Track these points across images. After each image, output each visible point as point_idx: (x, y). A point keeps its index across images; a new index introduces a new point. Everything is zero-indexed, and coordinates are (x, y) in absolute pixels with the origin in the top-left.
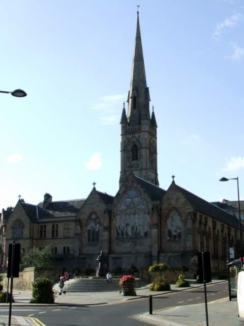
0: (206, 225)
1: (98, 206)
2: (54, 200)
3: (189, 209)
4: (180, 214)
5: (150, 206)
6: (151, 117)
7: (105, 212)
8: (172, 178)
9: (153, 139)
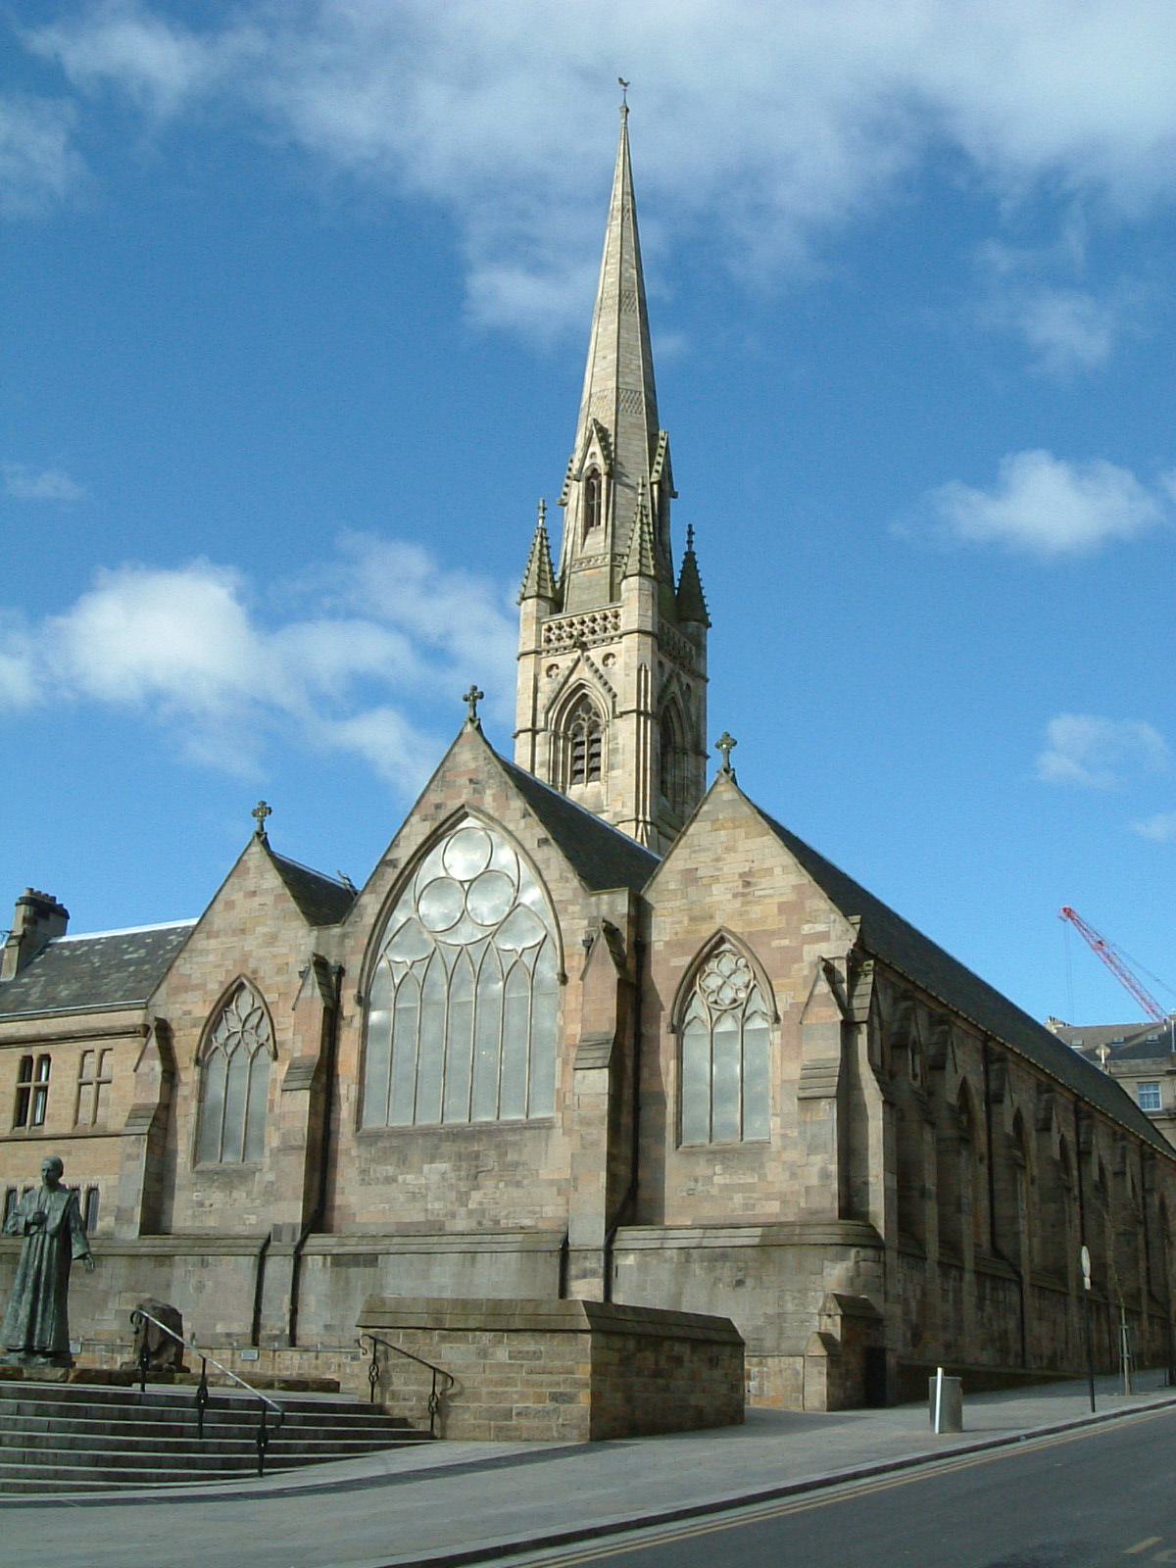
0: (937, 1066)
1: (272, 939)
3: (823, 937)
5: (577, 928)
6: (677, 575)
9: (685, 679)
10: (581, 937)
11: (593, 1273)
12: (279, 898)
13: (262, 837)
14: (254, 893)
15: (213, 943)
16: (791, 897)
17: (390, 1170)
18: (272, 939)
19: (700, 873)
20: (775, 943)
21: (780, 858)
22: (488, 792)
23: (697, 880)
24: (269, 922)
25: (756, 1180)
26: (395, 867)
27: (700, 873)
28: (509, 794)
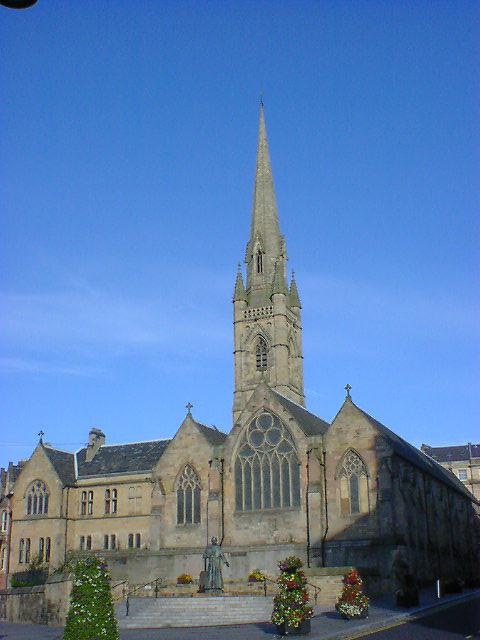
1: (198, 450)
2: (109, 443)
12: (198, 436)
13: (189, 415)
14: (189, 435)
18: (198, 450)
21: (366, 425)
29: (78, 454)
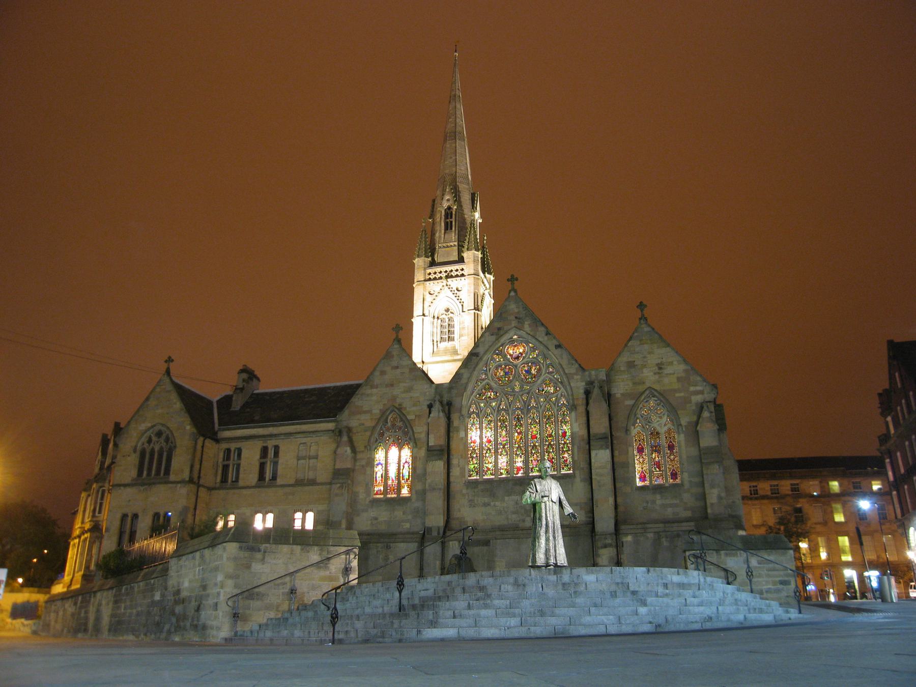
2: (264, 387)
3: (701, 392)
4: (673, 411)
7: (430, 407)
8: (639, 311)
10: (582, 391)
11: (610, 545)
14: (397, 367)
15: (375, 391)
16: (683, 375)
17: (486, 500)
18: (410, 389)
19: (636, 363)
20: (677, 395)
22: (526, 323)
23: (634, 366)
24: (407, 381)
25: (678, 502)
26: (478, 356)
27: (636, 363)
28: (538, 325)
29: (218, 402)
